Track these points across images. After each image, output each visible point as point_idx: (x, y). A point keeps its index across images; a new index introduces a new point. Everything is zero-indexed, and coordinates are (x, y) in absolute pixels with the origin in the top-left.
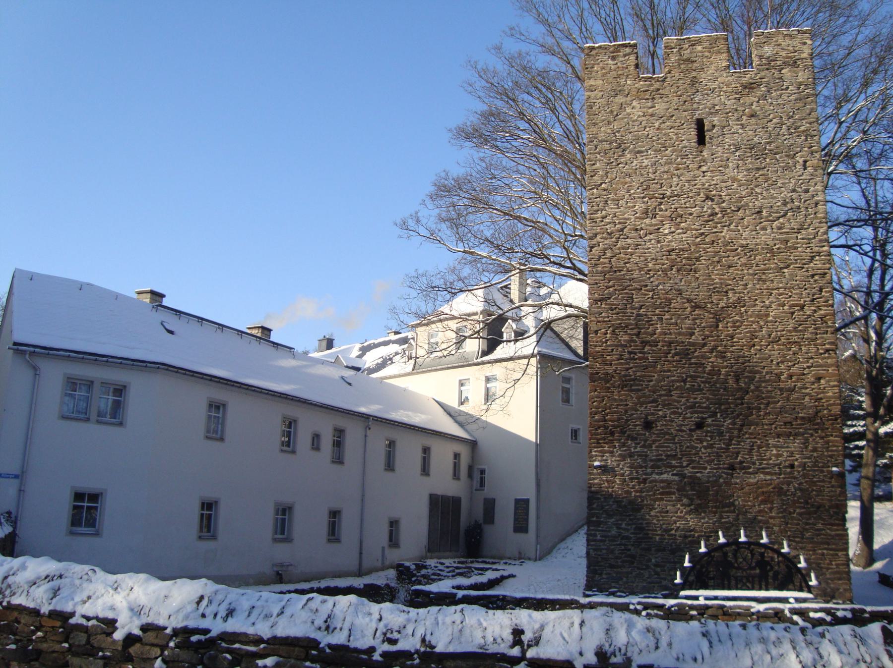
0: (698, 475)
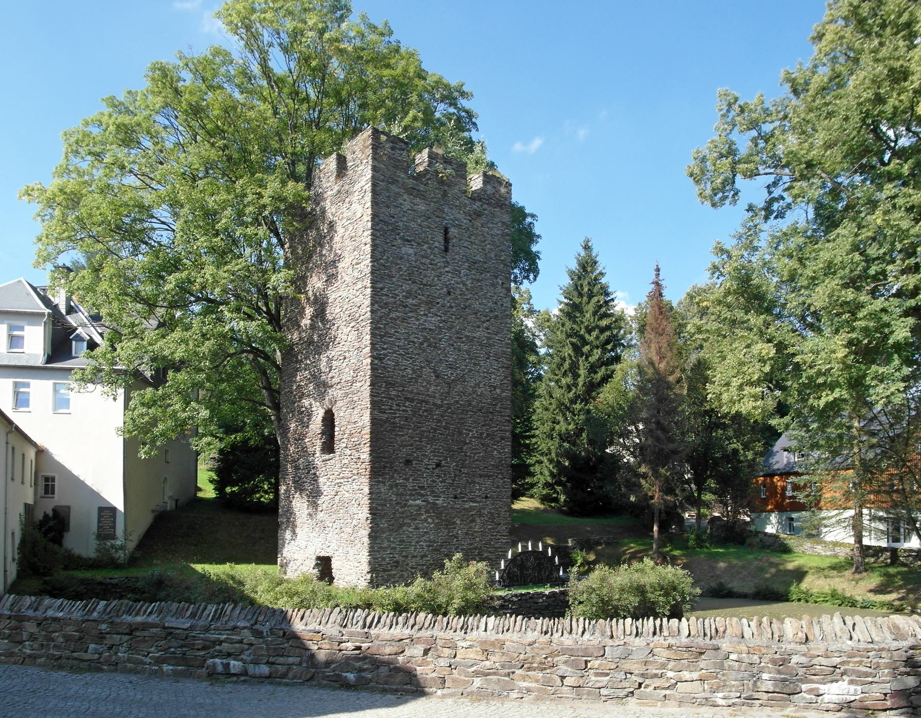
0: (437, 502)
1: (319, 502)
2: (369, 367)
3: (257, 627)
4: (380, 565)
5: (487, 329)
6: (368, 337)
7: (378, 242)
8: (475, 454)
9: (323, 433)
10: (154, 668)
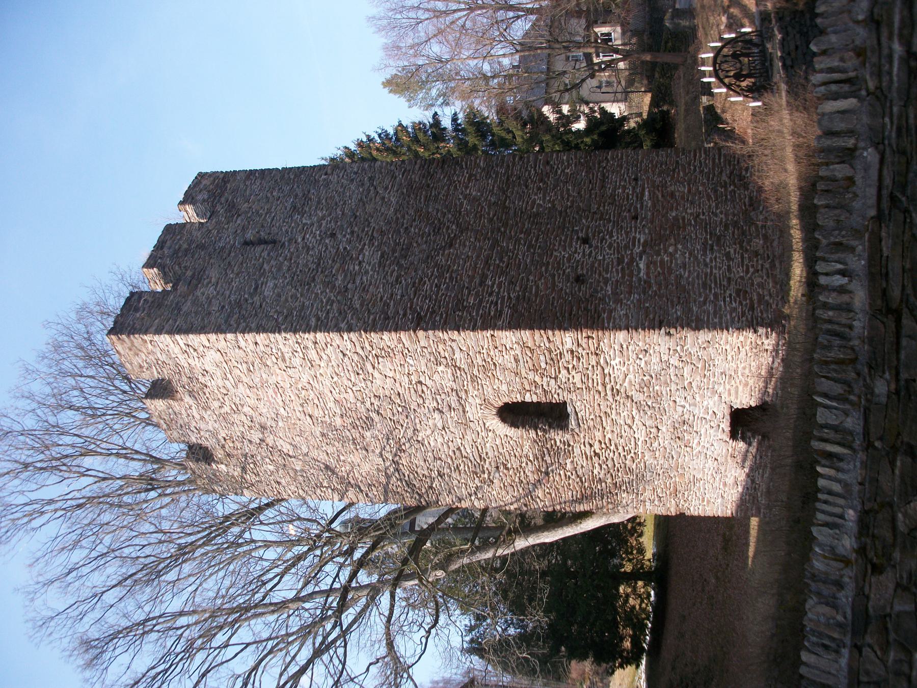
0: (642, 240)
2: (430, 332)
4: (743, 314)
6: (386, 336)
8: (569, 195)
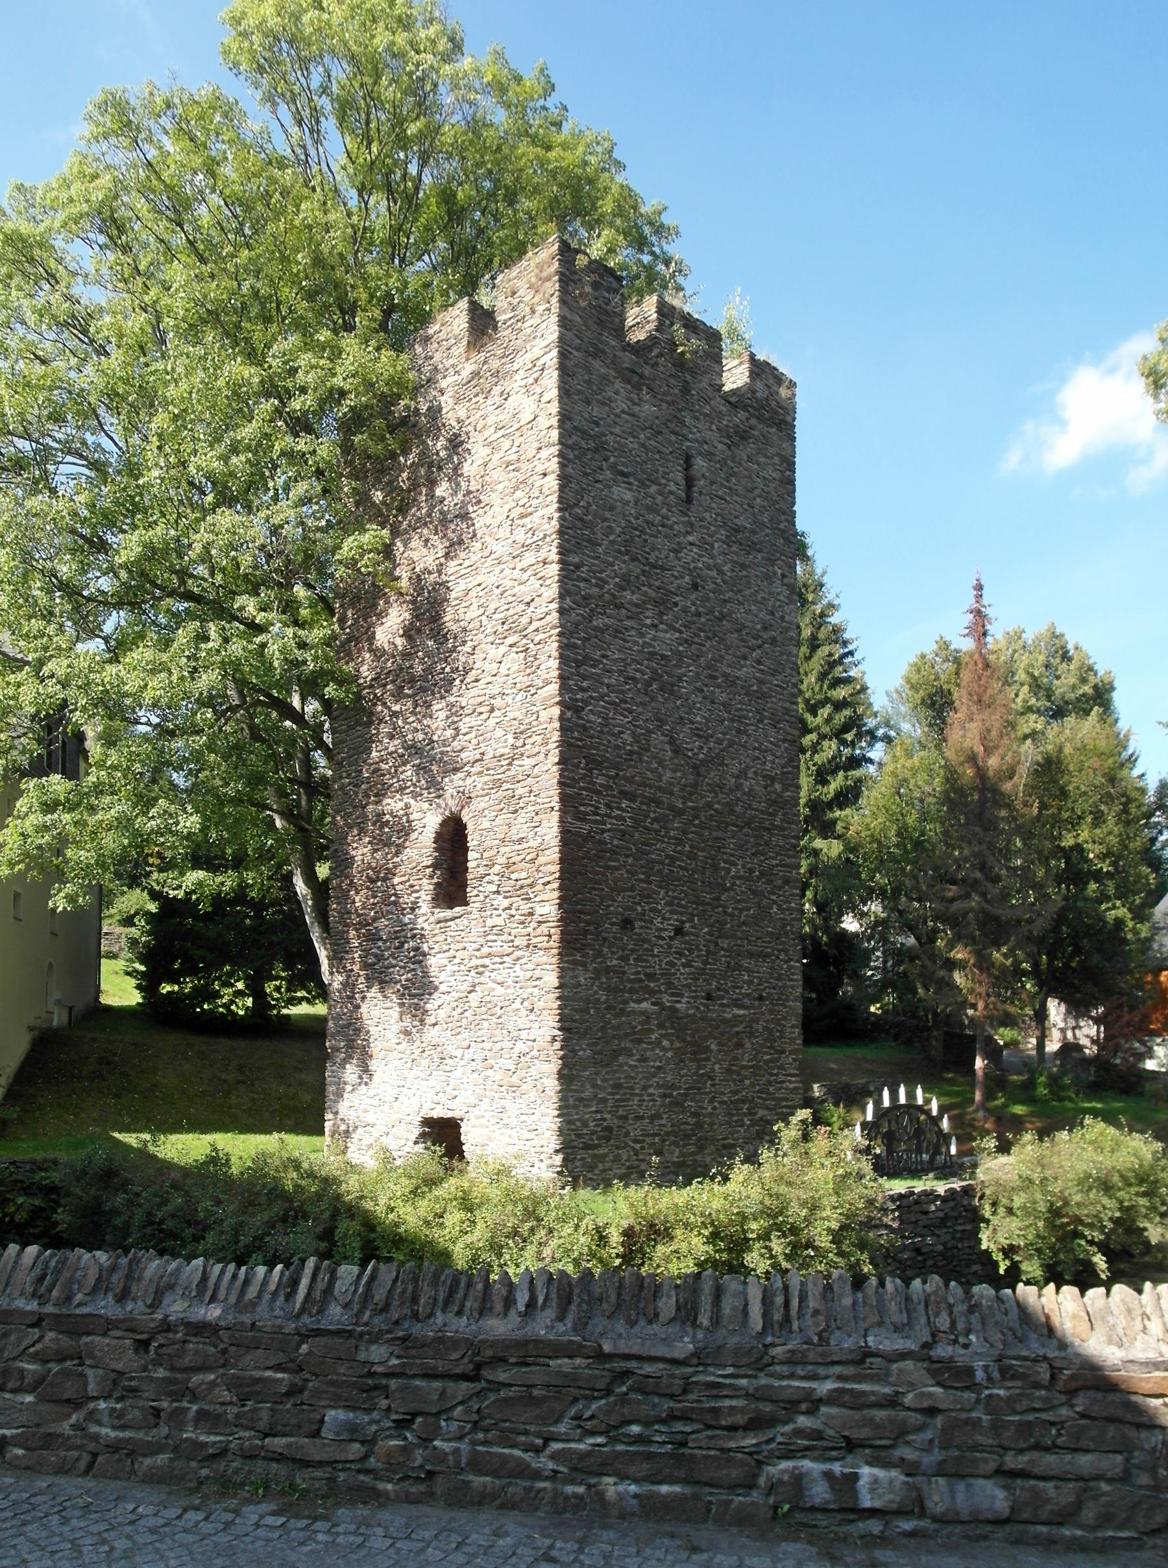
1: (428, 1006)
2: (557, 725)
3: (943, 1351)
4: (579, 1136)
5: (759, 662)
6: (554, 663)
7: (569, 470)
8: (741, 910)
9: (435, 866)
10: (569, 1489)
